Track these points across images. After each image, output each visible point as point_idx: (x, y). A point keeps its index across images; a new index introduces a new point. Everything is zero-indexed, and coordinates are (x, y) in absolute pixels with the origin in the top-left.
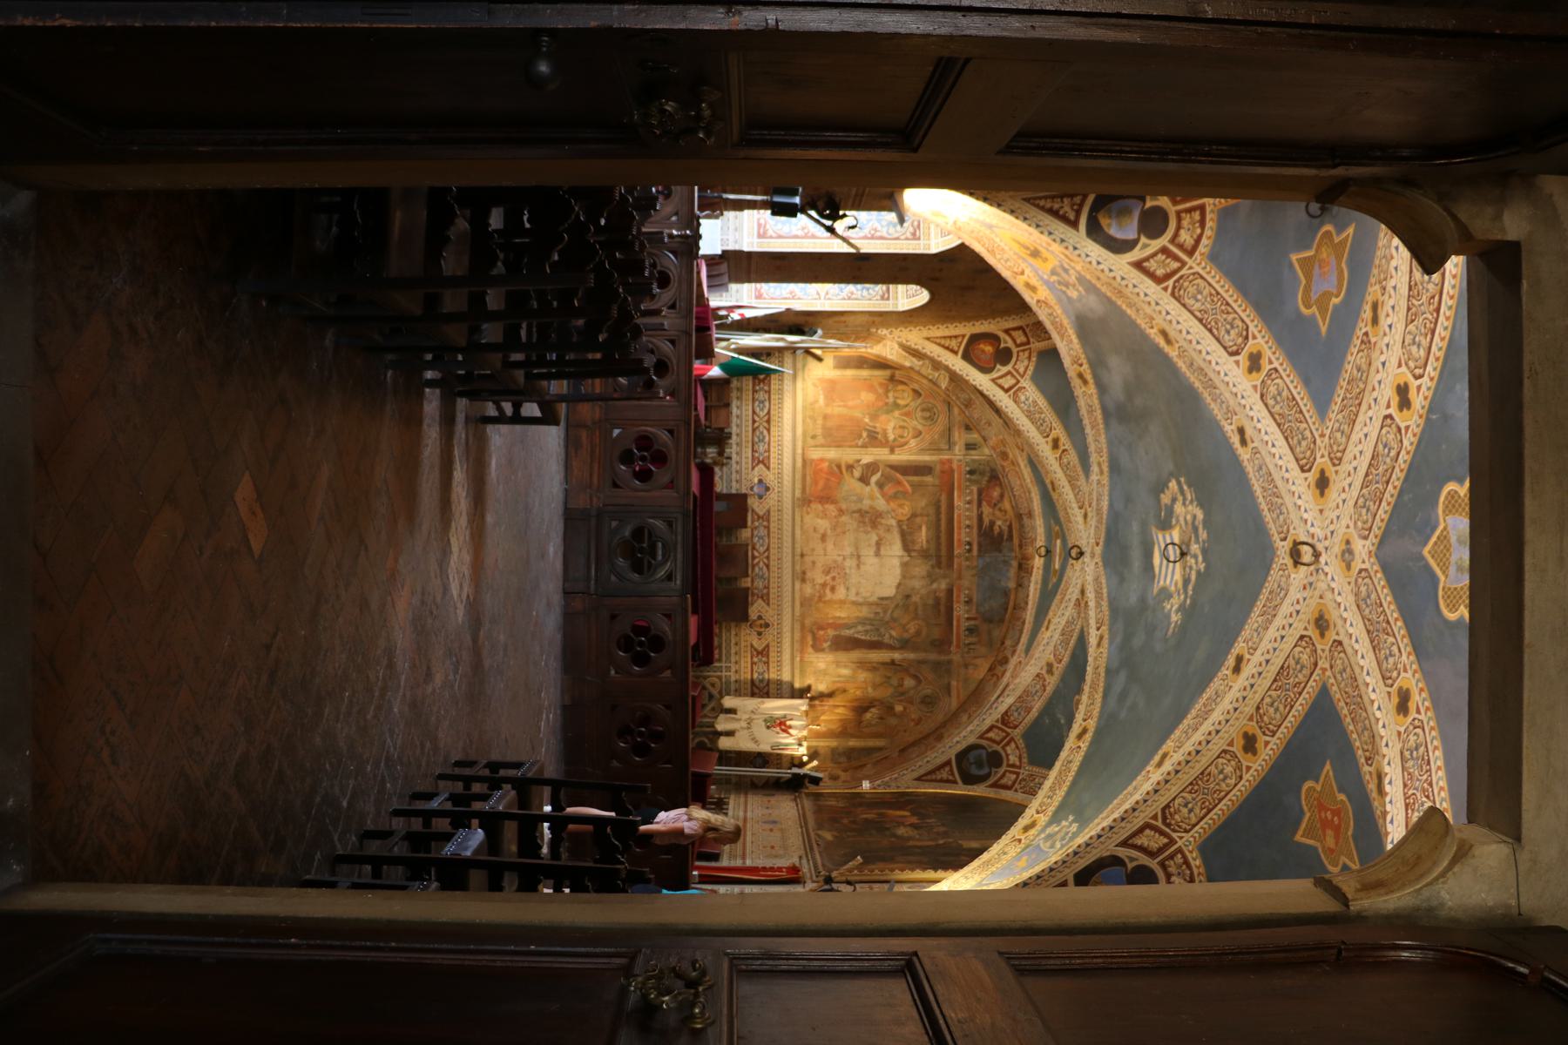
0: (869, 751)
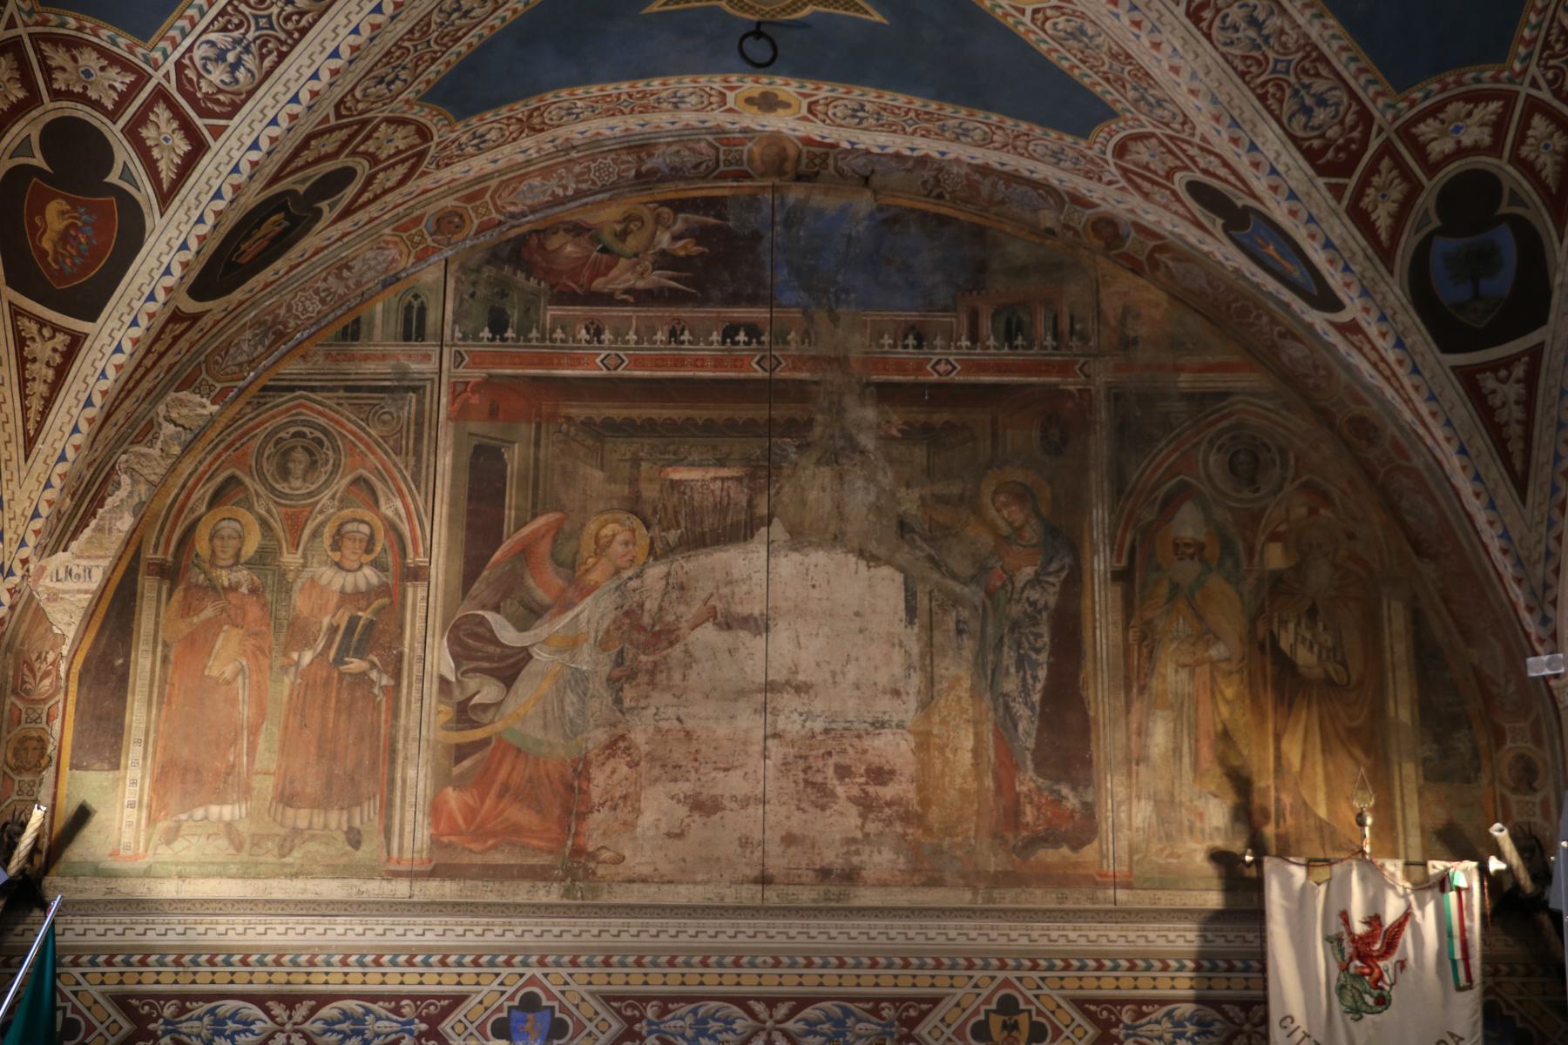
0: (1427, 659)
